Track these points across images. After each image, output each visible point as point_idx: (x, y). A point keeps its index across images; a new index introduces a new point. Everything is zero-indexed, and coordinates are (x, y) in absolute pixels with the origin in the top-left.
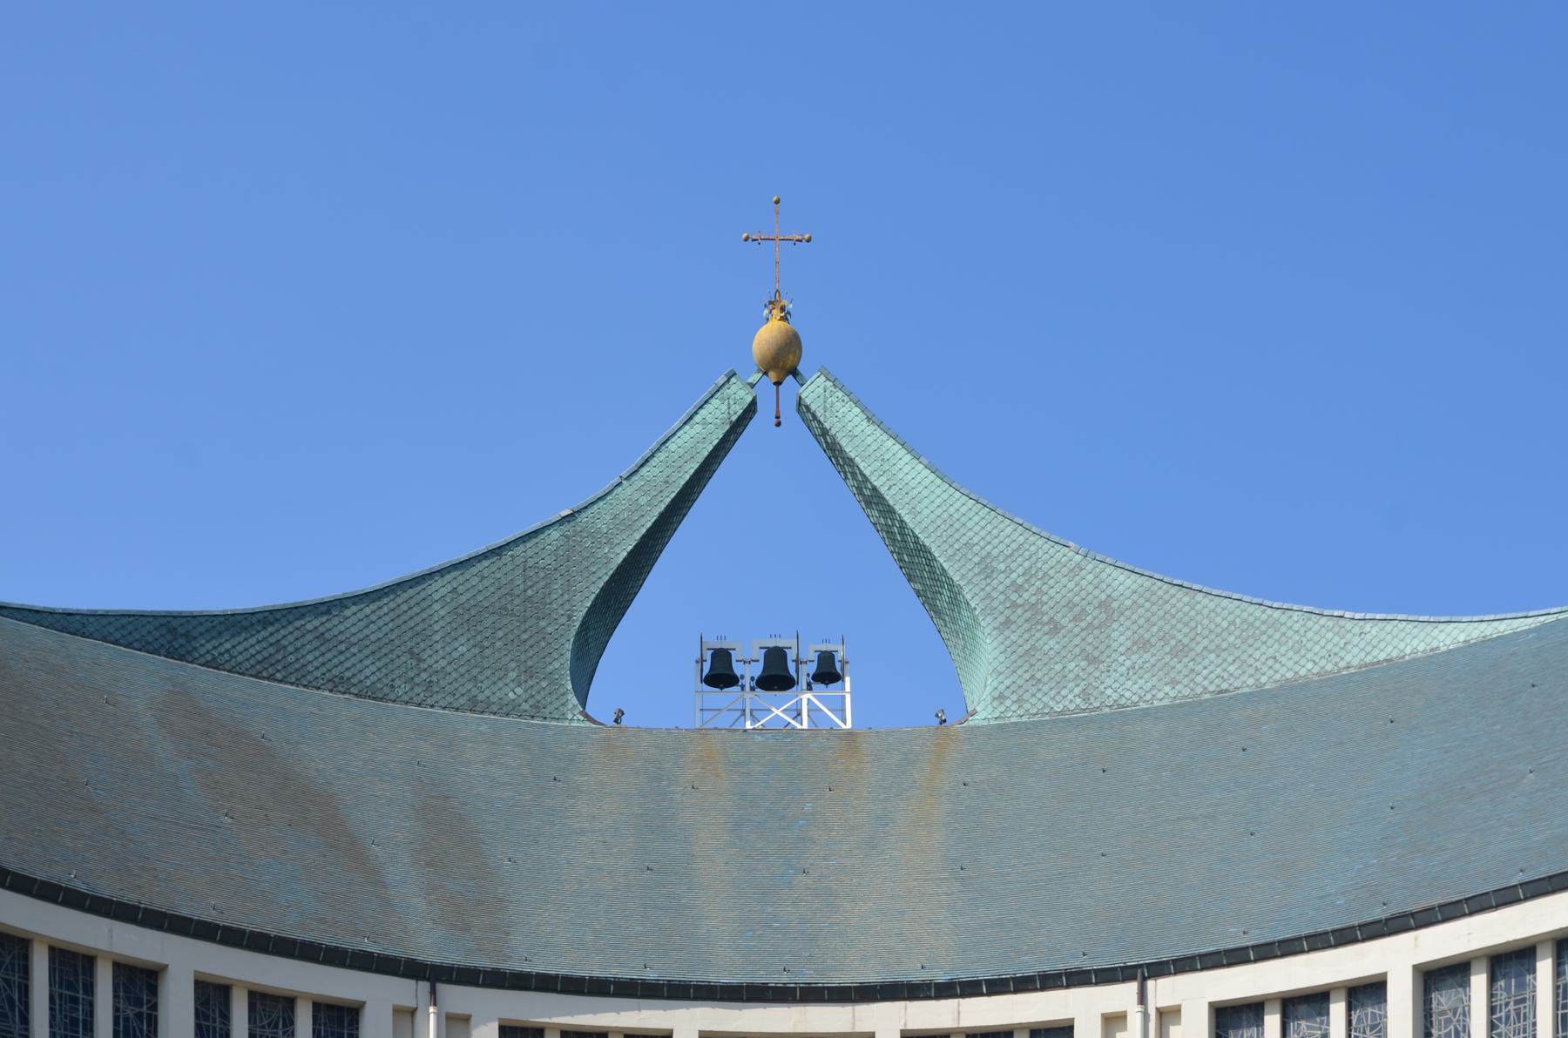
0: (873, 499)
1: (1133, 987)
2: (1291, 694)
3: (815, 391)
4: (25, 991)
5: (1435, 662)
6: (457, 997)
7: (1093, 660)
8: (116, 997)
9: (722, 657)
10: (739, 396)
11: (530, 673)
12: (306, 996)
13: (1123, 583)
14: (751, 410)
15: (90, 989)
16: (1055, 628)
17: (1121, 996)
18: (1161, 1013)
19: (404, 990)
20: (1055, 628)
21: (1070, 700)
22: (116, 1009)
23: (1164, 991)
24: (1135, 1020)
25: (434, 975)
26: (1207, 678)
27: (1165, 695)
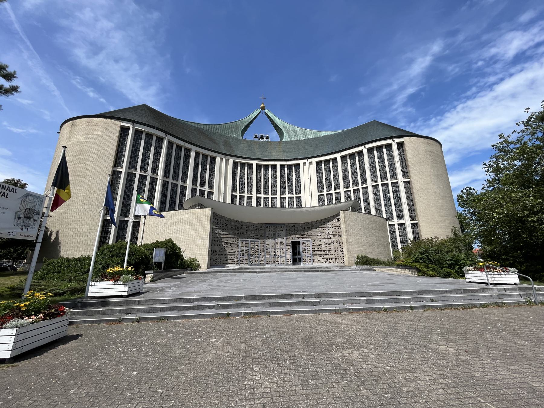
0: (272, 121)
1: (307, 160)
2: (316, 138)
3: (267, 111)
4: (172, 149)
5: (331, 135)
6: (228, 157)
7: (295, 136)
8: (185, 152)
9: (256, 136)
10: (259, 111)
11: (237, 134)
12: (209, 155)
13: (298, 129)
14: (260, 112)
15: (181, 150)
16: (291, 133)
17: (305, 161)
18: (310, 162)
19: (222, 156)
20: (291, 133)
21: (293, 139)
22: (184, 153)
23: (310, 160)
24: (307, 164)
25: (226, 155)
26: (307, 137)
27: (303, 139)
